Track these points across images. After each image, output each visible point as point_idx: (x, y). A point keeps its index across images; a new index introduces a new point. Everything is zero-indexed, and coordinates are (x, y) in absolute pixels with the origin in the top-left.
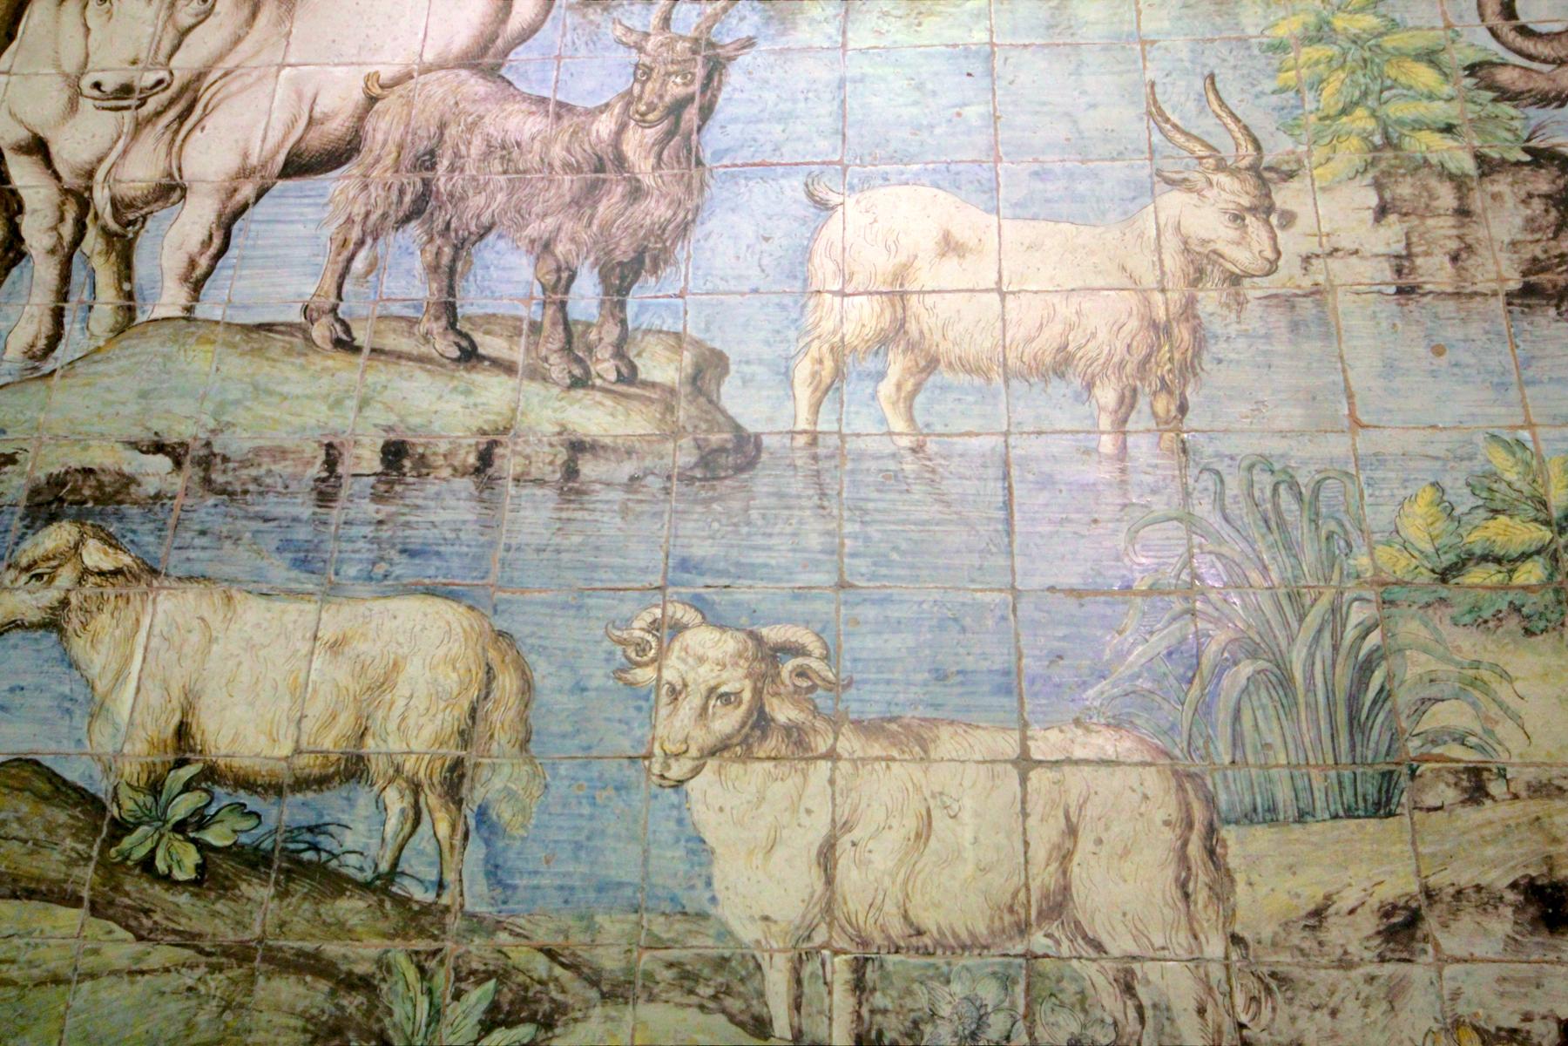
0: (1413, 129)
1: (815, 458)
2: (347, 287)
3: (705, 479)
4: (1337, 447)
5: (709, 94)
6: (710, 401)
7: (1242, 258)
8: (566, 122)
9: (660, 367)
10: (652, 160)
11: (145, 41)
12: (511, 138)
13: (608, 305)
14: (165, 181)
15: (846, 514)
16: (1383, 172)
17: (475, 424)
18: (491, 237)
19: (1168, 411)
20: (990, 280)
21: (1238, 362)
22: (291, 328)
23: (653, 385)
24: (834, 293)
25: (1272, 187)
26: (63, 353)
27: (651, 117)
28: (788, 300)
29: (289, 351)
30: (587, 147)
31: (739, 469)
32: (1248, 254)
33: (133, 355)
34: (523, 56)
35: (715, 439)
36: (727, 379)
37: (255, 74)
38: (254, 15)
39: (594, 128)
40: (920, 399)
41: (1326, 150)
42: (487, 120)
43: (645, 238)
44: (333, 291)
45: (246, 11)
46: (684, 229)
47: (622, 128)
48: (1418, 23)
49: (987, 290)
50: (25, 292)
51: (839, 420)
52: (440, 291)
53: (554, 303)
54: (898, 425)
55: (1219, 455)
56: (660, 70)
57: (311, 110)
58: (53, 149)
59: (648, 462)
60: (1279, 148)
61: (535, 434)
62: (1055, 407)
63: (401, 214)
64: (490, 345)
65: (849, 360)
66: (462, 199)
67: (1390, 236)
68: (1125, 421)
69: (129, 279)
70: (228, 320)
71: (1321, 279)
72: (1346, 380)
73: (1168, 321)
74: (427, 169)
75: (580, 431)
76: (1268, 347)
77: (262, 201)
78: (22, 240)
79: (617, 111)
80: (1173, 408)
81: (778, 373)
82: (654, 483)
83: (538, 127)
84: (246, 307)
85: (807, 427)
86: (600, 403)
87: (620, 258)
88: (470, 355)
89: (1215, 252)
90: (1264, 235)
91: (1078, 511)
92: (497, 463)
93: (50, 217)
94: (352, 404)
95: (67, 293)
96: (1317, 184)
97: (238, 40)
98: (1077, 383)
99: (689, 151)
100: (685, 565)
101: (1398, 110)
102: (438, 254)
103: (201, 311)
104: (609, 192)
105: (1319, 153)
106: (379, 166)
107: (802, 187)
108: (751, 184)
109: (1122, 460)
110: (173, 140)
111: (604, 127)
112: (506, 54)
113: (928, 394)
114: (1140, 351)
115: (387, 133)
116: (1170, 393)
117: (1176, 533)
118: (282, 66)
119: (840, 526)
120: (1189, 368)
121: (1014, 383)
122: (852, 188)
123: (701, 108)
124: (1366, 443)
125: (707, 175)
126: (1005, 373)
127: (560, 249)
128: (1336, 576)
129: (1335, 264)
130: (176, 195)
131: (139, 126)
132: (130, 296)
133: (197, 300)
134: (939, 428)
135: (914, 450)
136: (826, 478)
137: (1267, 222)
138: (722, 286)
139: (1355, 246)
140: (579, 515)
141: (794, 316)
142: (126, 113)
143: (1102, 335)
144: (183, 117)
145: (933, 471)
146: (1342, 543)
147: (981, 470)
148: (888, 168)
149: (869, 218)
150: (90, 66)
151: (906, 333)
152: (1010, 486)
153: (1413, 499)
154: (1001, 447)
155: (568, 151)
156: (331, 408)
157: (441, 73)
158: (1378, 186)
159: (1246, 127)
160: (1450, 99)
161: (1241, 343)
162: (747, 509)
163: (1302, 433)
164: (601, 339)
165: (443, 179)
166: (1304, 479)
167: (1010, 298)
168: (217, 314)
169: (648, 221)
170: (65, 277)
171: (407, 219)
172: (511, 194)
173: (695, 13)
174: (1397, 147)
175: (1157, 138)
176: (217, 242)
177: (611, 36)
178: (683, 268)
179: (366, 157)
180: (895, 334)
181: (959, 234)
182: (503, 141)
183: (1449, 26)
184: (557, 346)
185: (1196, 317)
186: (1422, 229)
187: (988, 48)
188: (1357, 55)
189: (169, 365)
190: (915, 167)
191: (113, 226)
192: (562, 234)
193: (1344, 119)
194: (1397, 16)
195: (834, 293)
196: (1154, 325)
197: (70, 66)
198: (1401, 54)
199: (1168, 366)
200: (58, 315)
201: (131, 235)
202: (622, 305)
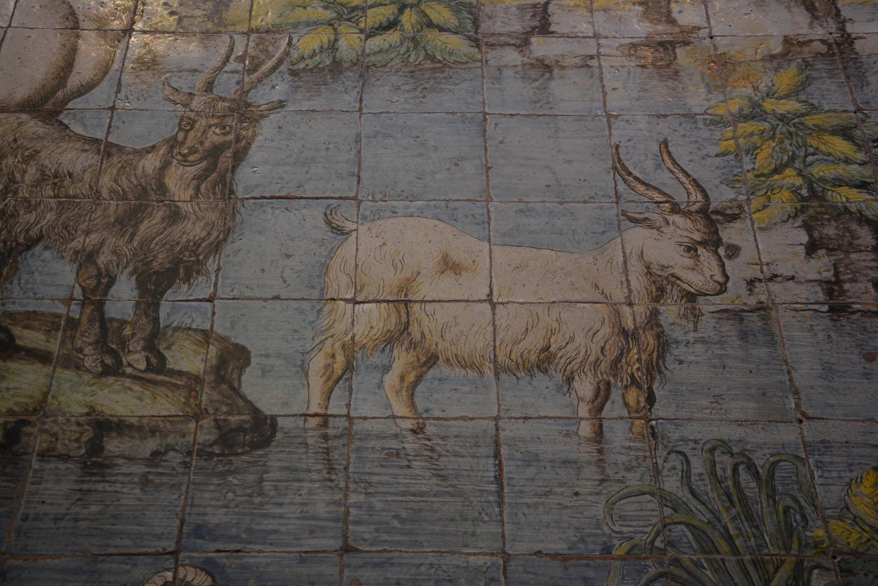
0: (834, 185)
1: (326, 437)
3: (222, 455)
4: (788, 434)
5: (244, 143)
6: (232, 388)
7: (696, 280)
8: (115, 159)
9: (187, 358)
10: (190, 192)
12: (65, 168)
13: (143, 306)
15: (352, 486)
16: (810, 217)
18: (38, 248)
19: (638, 402)
20: (483, 294)
21: (697, 363)
23: (180, 373)
24: (346, 300)
25: (719, 226)
27: (191, 158)
28: (305, 305)
30: (133, 179)
31: (254, 446)
32: (701, 278)
34: (80, 106)
35: (234, 419)
36: (248, 369)
39: (141, 164)
40: (420, 388)
41: (763, 200)
42: (42, 154)
43: (180, 252)
46: (217, 247)
47: (165, 166)
48: (833, 107)
49: (480, 301)
51: (348, 405)
54: (401, 409)
55: (685, 440)
56: (201, 123)
59: (170, 440)
60: (722, 196)
61: (64, 414)
62: (541, 397)
65: (359, 355)
67: (820, 266)
68: (601, 409)
71: (764, 298)
72: (791, 380)
73: (636, 328)
75: (107, 411)
76: (723, 352)
79: (162, 152)
80: (642, 399)
82: (174, 458)
83: (90, 162)
85: (319, 411)
89: (673, 275)
90: (714, 264)
91: (561, 485)
92: (24, 439)
96: (756, 226)
98: (559, 377)
99: (224, 185)
100: (200, 531)
101: (819, 171)
104: (151, 215)
105: (756, 203)
107: (321, 217)
108: (277, 212)
109: (600, 442)
111: (150, 163)
113: (428, 384)
114: (612, 353)
116: (639, 387)
117: (650, 506)
119: (346, 496)
120: (654, 368)
121: (503, 376)
122: (365, 218)
124: (810, 431)
125: (239, 204)
126: (496, 368)
127: (102, 260)
128: (795, 546)
129: (774, 287)
134: (437, 413)
135: (414, 432)
136: (335, 455)
137: (716, 253)
138: (248, 293)
139: (791, 273)
140: (100, 487)
141: (311, 318)
143: (580, 339)
145: (432, 450)
146: (798, 517)
147: (475, 449)
148: (395, 203)
149: (378, 242)
151: (409, 334)
152: (500, 462)
153: (859, 481)
154: (491, 430)
155: (116, 181)
158: (807, 227)
159: (694, 180)
160: (863, 164)
161: (699, 348)
162: (261, 481)
163: (755, 423)
164: (134, 335)
166: (760, 461)
167: (499, 308)
169: (184, 239)
172: (59, 215)
173: (234, 81)
174: (822, 198)
175: (621, 187)
180: (399, 335)
181: (454, 256)
182: (57, 171)
183: (859, 110)
184: (92, 339)
185: (659, 325)
186: (847, 261)
187: (481, 116)
188: (784, 129)
193: (776, 177)
194: (815, 102)
195: (346, 300)
196: (624, 333)
198: (819, 130)
199: (637, 365)
202: (156, 306)
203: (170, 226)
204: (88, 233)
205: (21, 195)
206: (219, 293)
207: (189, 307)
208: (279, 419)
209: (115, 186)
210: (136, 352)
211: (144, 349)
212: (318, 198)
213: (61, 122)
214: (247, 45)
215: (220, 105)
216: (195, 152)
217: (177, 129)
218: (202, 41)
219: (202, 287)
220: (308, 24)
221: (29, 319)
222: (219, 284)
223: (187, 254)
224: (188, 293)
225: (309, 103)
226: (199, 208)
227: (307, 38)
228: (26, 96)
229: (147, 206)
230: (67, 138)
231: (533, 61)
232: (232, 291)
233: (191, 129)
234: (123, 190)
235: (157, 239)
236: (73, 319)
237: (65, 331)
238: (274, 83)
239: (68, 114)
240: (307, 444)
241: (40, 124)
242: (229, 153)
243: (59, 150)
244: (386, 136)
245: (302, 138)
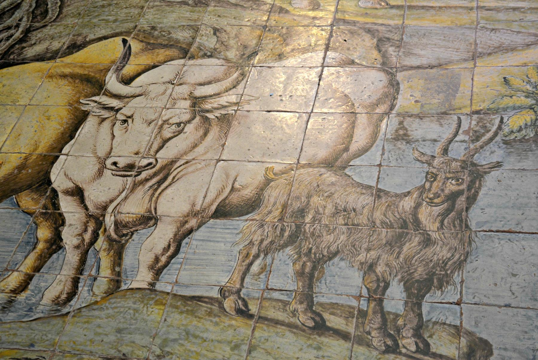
2: (247, 280)
5: (473, 191)
10: (437, 224)
11: (144, 144)
14: (146, 214)
18: (336, 259)
22: (211, 300)
26: (75, 304)
29: (210, 313)
30: (396, 214)
33: (116, 307)
38: (205, 134)
43: (433, 267)
45: (201, 132)
46: (460, 265)
47: (418, 206)
50: (58, 268)
52: (303, 287)
53: (375, 300)
57: (233, 184)
58: (86, 194)
63: (282, 242)
66: (319, 236)
69: (120, 265)
70: (175, 292)
77: (202, 229)
78: (62, 240)
84: (187, 286)
87: (418, 278)
93: (79, 228)
95: (82, 270)
97: (195, 146)
99: (461, 221)
102: (304, 265)
103: (159, 286)
104: (410, 240)
106: (271, 215)
108: (502, 242)
110: (153, 194)
115: (276, 198)
118: (218, 161)
125: (473, 235)
127: (379, 269)
130: (153, 221)
131: (135, 186)
132: (119, 274)
133: (158, 280)
142: (129, 178)
144: (160, 183)
150: (112, 154)
155: (385, 215)
168: (168, 289)
169: (435, 258)
170: (83, 261)
171: (285, 246)
176: (172, 249)
177: (412, 157)
178: (459, 287)
179: (263, 210)
189: (137, 315)
191: (114, 235)
197: (102, 153)
200: (76, 282)
201: (123, 242)
203: (425, 248)
204: (368, 250)
205: (323, 222)
206: (464, 299)
207: (443, 308)
209: (384, 219)
211: (414, 336)
212: (533, 233)
213: (346, 174)
214: (470, 123)
215: (454, 164)
216: (438, 197)
217: (424, 180)
218: (438, 120)
219: (451, 294)
220: (514, 108)
221: (334, 308)
223: (439, 269)
225: (520, 164)
226: (445, 237)
227: (515, 118)
229: (407, 234)
230: (351, 185)
232: (474, 298)
234: (390, 221)
235: (416, 257)
236: (363, 310)
237: (357, 318)
238: (493, 149)
239: (352, 168)
241: (333, 175)
242: (463, 198)
243: (346, 193)
245: (517, 189)
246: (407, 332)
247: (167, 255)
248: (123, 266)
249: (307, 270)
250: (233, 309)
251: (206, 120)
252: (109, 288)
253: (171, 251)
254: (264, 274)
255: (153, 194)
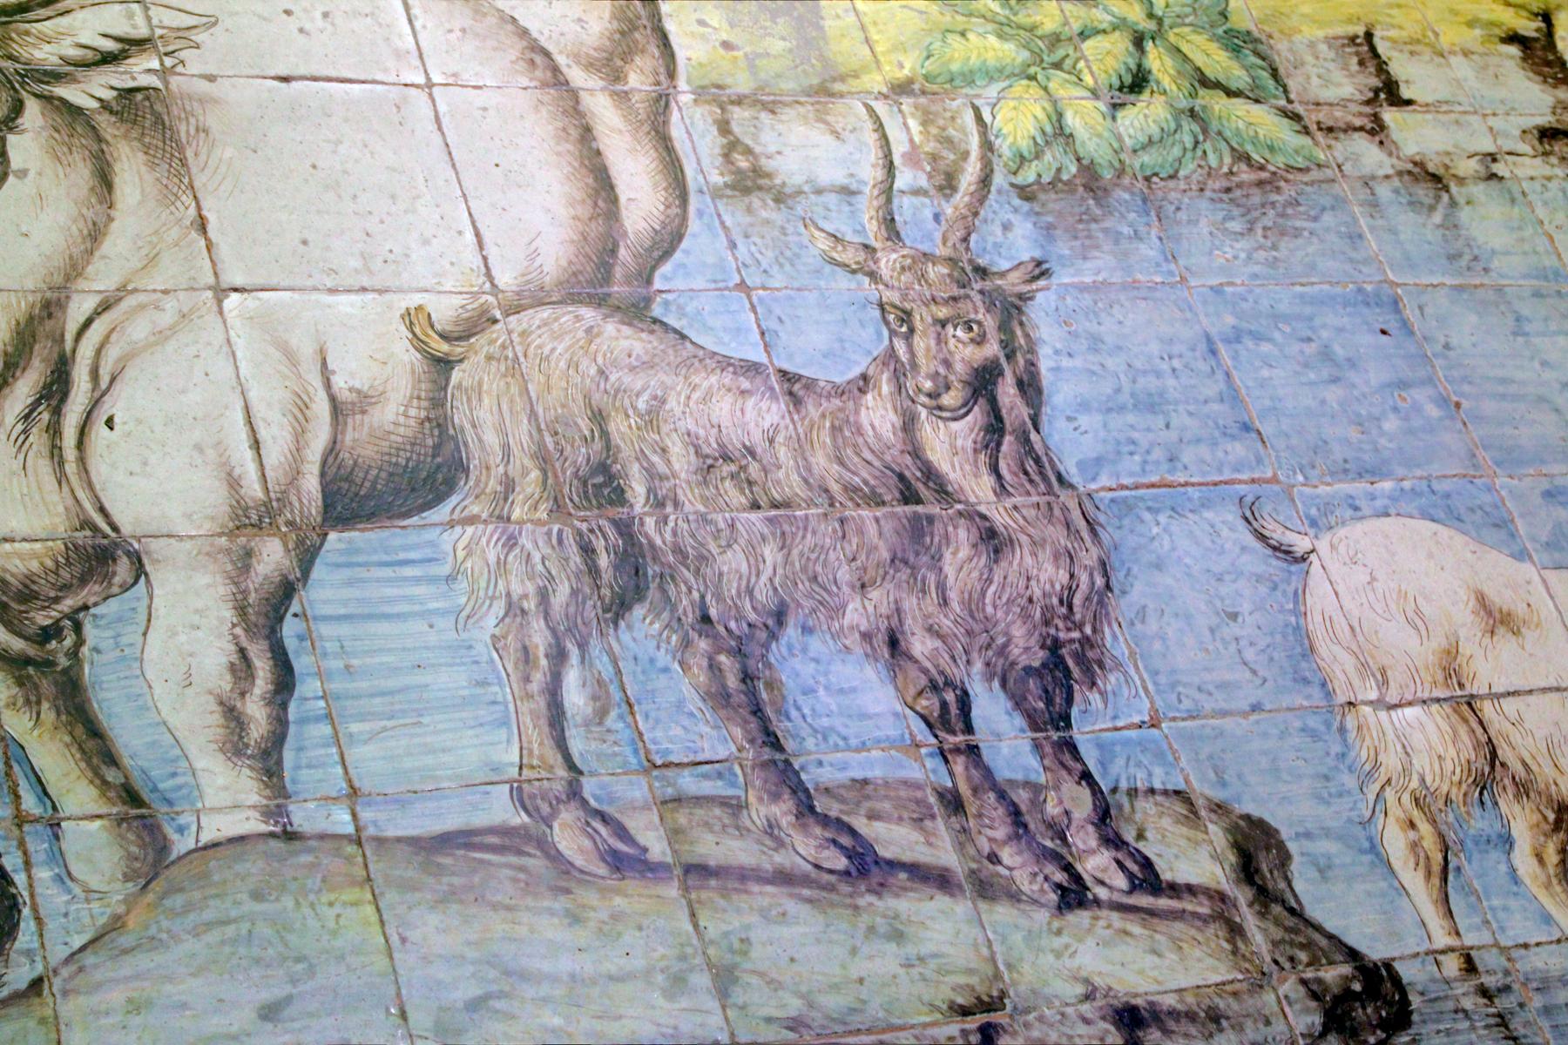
2: (576, 746)
6: (1292, 911)
8: (812, 410)
10: (988, 481)
13: (1048, 749)
17: (944, 993)
18: (791, 632)
22: (508, 840)
23: (1191, 890)
27: (948, 399)
30: (868, 455)
37: (170, 304)
38: (105, 180)
44: (555, 758)
45: (83, 174)
47: (909, 424)
64: (894, 838)
69: (112, 760)
74: (611, 503)
81: (1362, 851)
86: (1126, 933)
87: (1024, 661)
88: (865, 866)
94: (702, 980)
97: (95, 235)
99: (1037, 461)
102: (713, 667)
108: (1162, 518)
111: (878, 415)
112: (646, 276)
118: (221, 292)
123: (1020, 384)
141: (1336, 748)
155: (841, 463)
156: (669, 995)
157: (545, 313)
165: (650, 522)
168: (341, 821)
176: (263, 667)
180: (1490, 772)
190: (1387, 485)
192: (909, 621)
201: (63, 662)
203: (996, 561)
205: (688, 508)
208: (1397, 965)
210: (1093, 852)
222: (1150, 687)
224: (1110, 712)
228: (564, 263)
230: (696, 361)
231: (1410, 166)
233: (912, 330)
234: (866, 483)
240: (1465, 1011)
244: (1258, 337)
246: (1084, 838)
247: (257, 691)
248: (127, 761)
249: (732, 682)
250: (594, 856)
251: (74, 111)
252: (133, 858)
253: (261, 673)
254: (613, 714)
255: (55, 452)
